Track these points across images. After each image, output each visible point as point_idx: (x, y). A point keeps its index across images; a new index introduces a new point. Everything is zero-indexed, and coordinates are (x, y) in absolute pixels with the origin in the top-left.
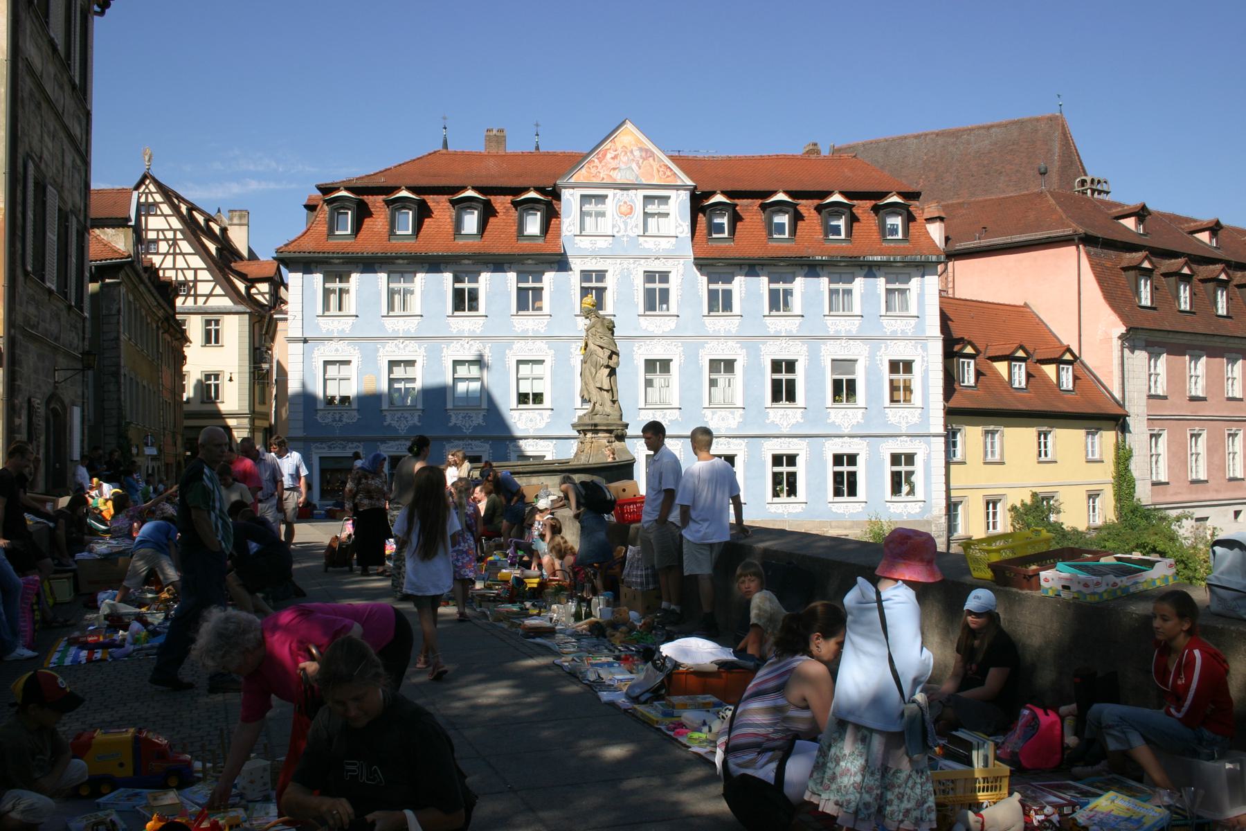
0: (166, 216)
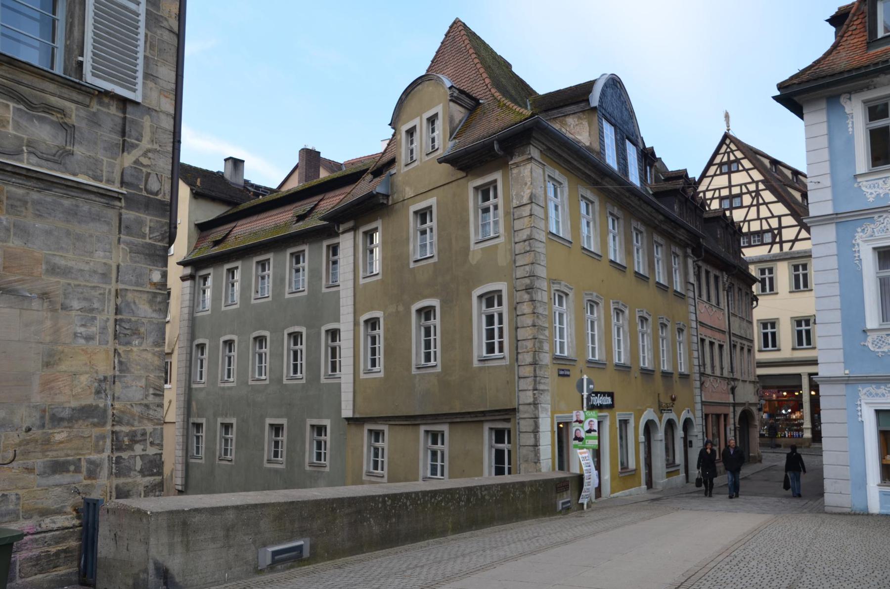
0: (747, 170)
